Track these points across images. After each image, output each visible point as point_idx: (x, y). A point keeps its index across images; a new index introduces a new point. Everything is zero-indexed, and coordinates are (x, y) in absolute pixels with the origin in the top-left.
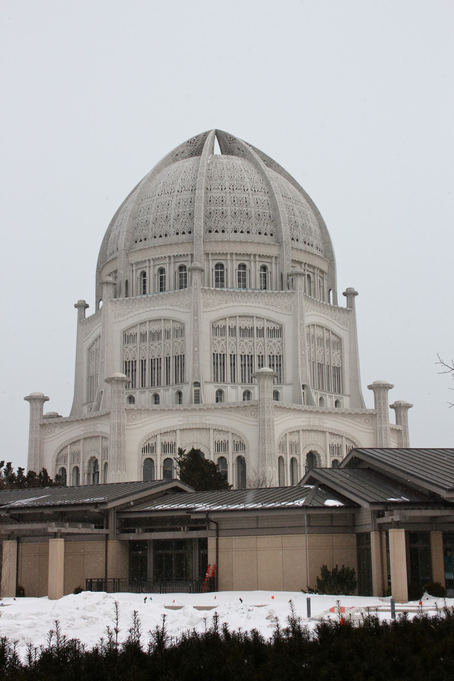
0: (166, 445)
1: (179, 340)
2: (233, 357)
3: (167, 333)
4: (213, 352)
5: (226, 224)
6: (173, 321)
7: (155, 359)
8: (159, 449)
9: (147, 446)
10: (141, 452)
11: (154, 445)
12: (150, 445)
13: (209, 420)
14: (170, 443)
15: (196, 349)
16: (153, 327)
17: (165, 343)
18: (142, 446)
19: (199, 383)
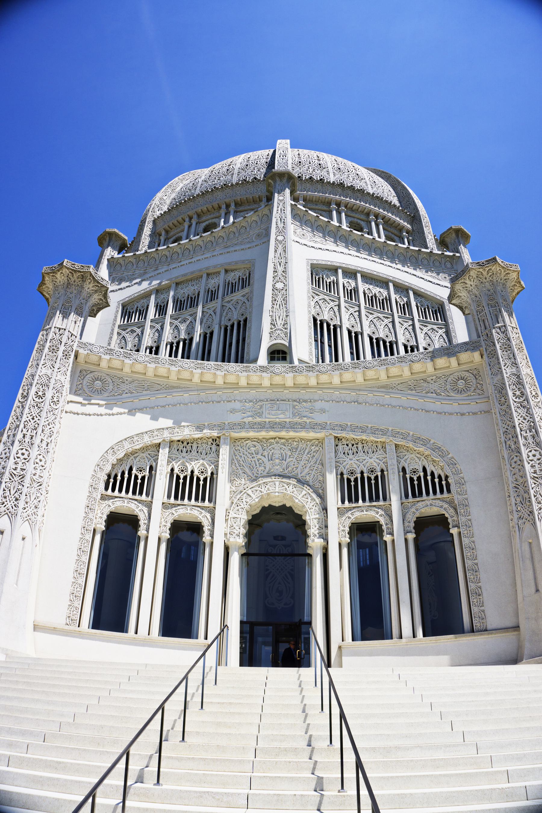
0: (185, 478)
1: (238, 295)
2: (355, 338)
3: (212, 295)
4: (313, 312)
5: (326, 174)
6: (226, 271)
7: (178, 343)
8: (161, 483)
9: (123, 473)
10: (102, 486)
11: (147, 473)
12: (134, 472)
13: (323, 411)
14: (196, 473)
15: (279, 286)
16: (182, 291)
17: (205, 309)
18: (108, 468)
19: (284, 353)
